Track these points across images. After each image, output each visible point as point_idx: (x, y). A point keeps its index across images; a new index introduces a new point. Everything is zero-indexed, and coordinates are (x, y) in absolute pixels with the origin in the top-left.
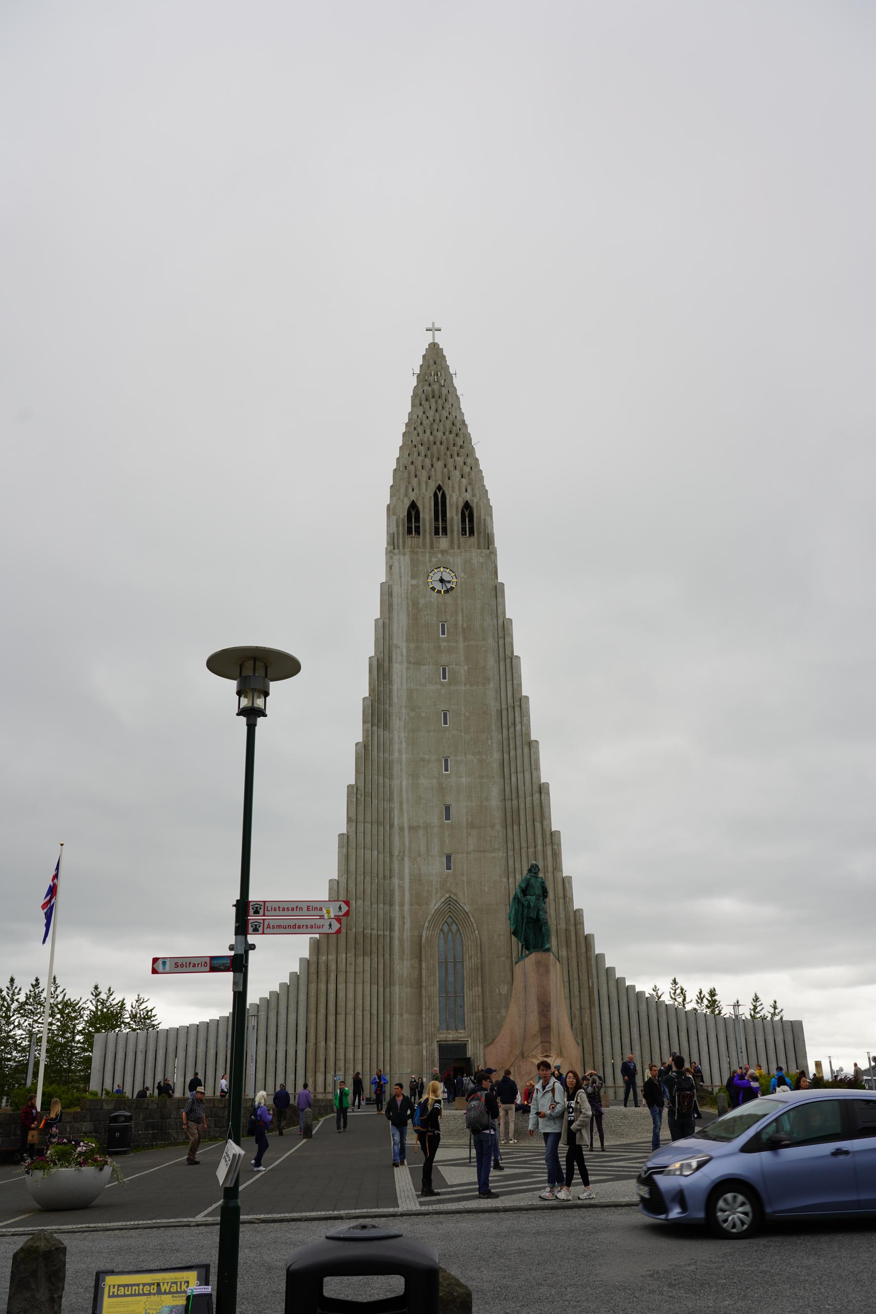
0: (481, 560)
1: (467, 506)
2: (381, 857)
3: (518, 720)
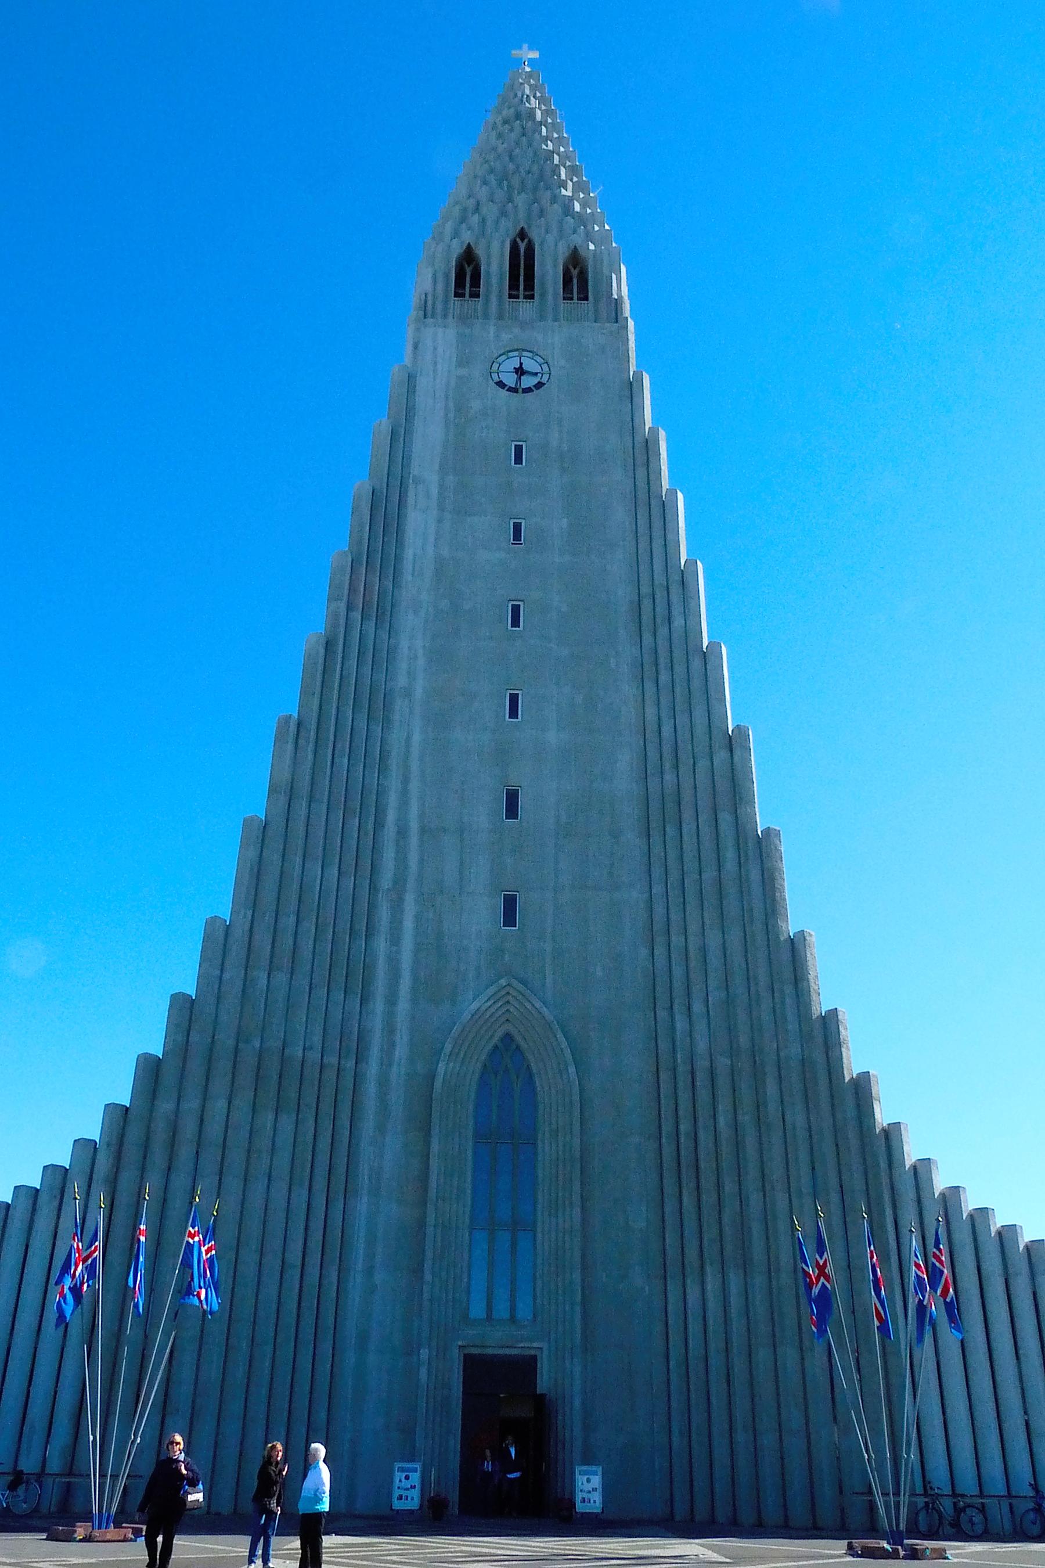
3: (677, 609)
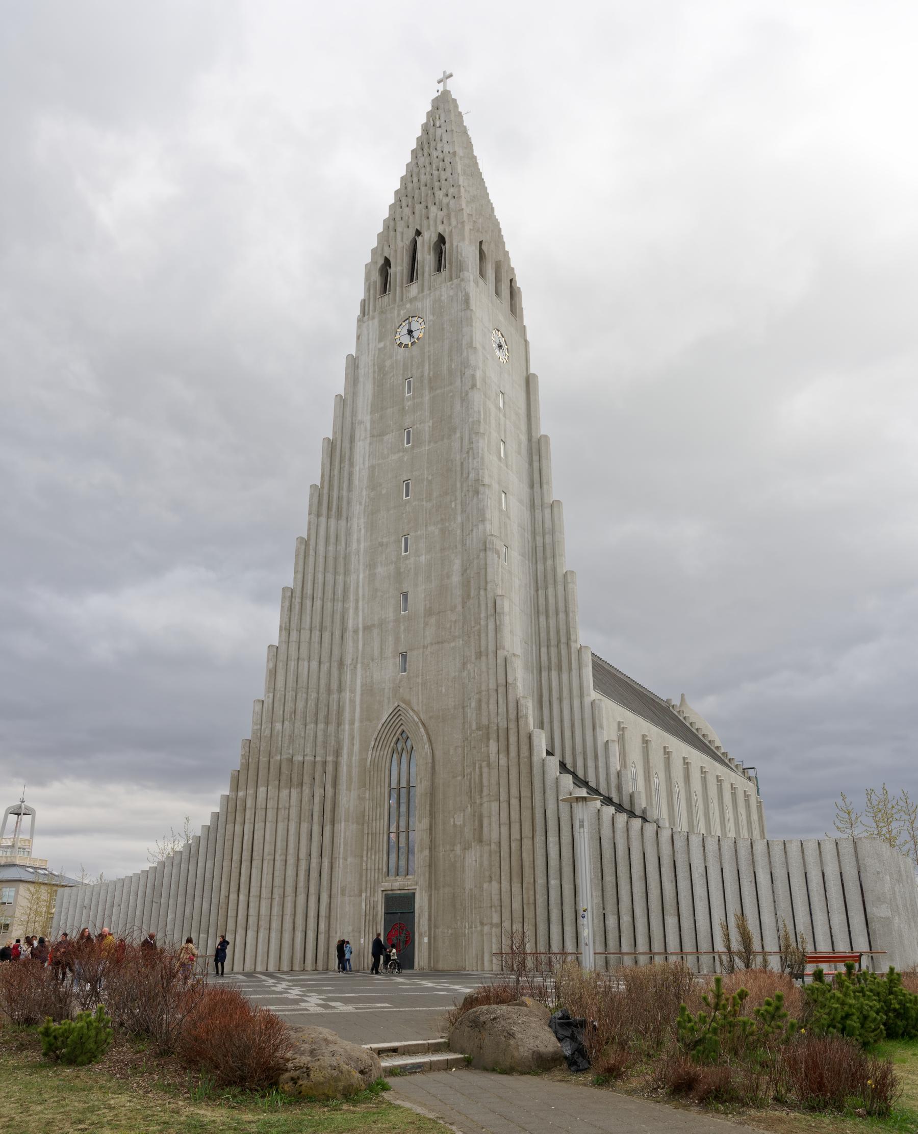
0: (451, 293)
2: (325, 667)
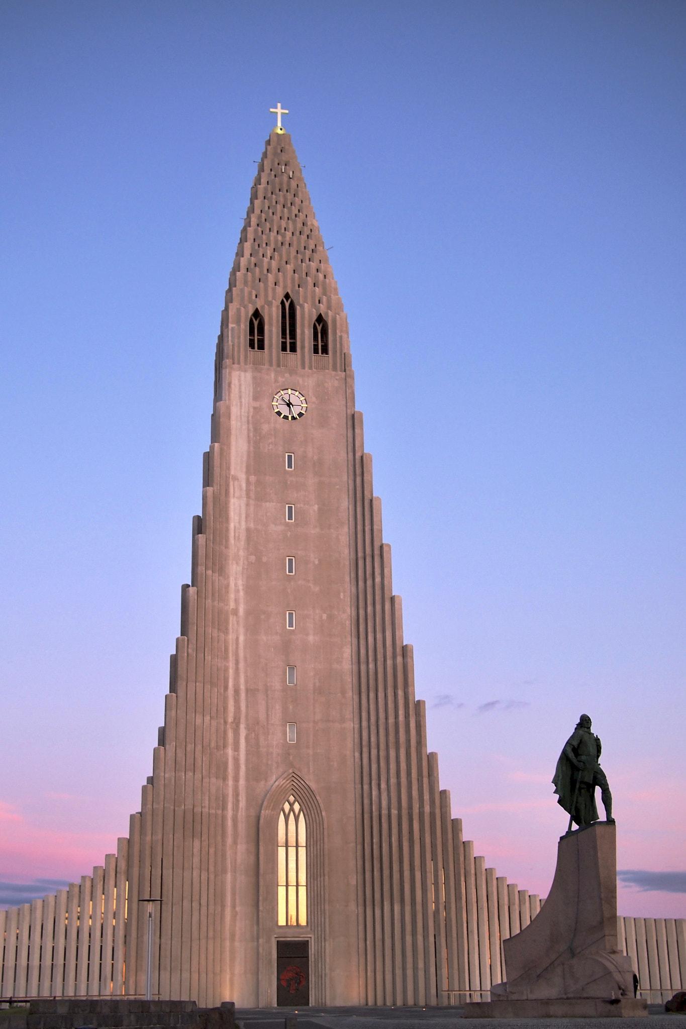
1: (320, 319)
2: (214, 723)
